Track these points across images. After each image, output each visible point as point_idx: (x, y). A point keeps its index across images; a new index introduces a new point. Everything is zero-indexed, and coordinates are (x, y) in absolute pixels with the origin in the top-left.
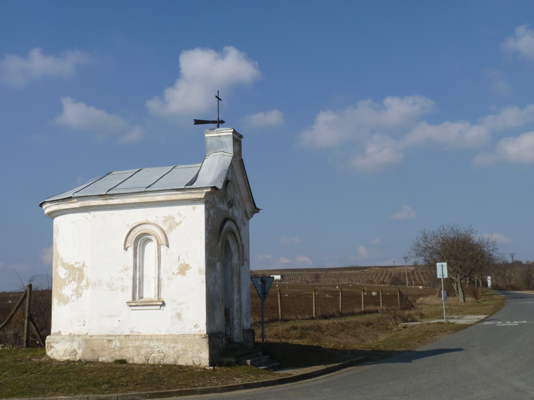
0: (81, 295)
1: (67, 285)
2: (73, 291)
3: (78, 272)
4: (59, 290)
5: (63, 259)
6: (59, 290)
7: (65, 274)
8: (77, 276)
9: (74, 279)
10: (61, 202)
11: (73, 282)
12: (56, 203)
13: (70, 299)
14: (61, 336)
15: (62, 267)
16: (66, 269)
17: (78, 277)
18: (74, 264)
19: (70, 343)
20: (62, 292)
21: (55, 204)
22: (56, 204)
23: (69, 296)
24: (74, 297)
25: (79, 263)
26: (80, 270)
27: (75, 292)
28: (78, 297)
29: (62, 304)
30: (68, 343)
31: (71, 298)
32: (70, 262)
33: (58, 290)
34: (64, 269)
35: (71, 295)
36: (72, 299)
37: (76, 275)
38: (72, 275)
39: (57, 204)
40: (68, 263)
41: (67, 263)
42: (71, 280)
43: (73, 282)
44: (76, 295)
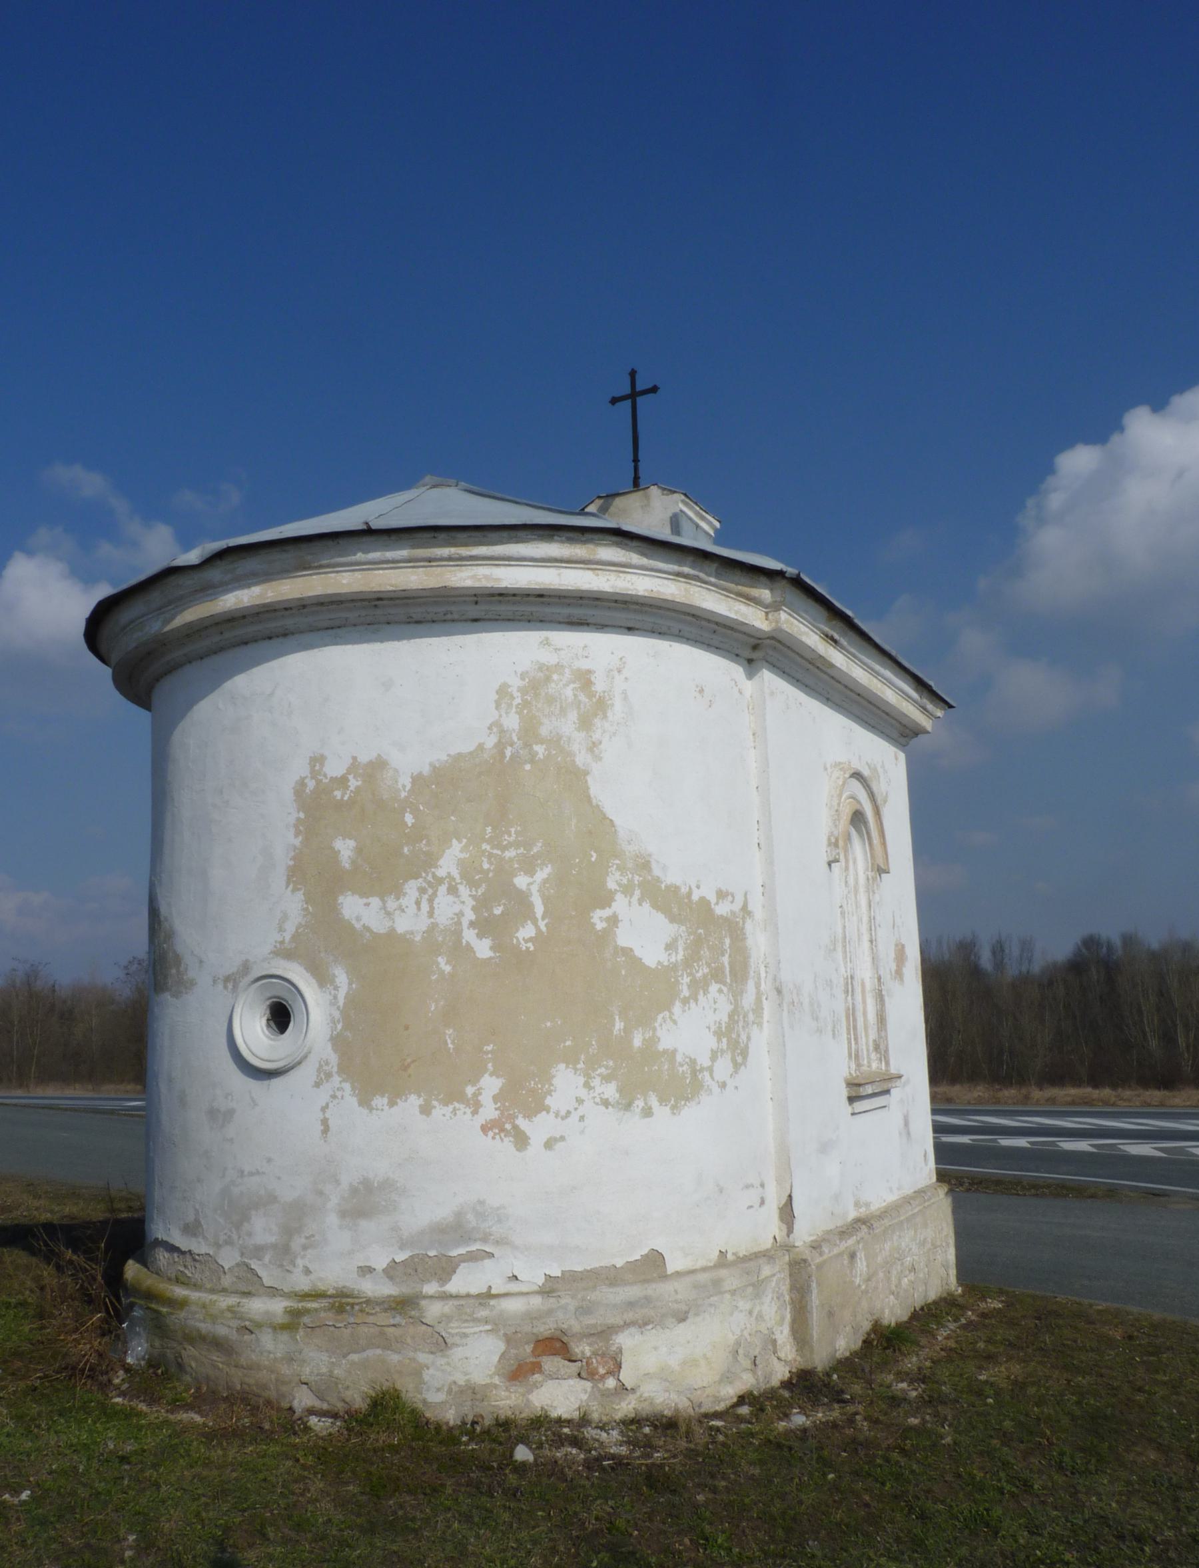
0: (745, 1053)
1: (685, 1001)
2: (719, 1034)
3: (727, 941)
4: (628, 1031)
5: (654, 865)
6: (628, 1031)
7: (670, 947)
8: (726, 960)
9: (717, 975)
10: (709, 575)
11: (714, 987)
12: (686, 570)
13: (706, 1074)
14: (664, 1277)
15: (647, 906)
16: (673, 919)
17: (730, 963)
18: (712, 898)
19: (748, 1306)
20: (651, 1042)
21: (675, 568)
22: (678, 574)
23: (704, 1060)
24: (723, 1067)
25: (730, 898)
26: (734, 928)
27: (724, 1040)
28: (737, 1066)
29: (654, 1101)
30: (741, 1304)
31: (710, 1070)
32: (694, 888)
33: (619, 1025)
34: (660, 918)
35: (709, 1054)
36: (716, 1079)
37: (723, 955)
38: (705, 953)
39: (686, 576)
40: (684, 890)
41: (677, 888)
42: (705, 976)
43: (714, 987)
44: (728, 1056)
